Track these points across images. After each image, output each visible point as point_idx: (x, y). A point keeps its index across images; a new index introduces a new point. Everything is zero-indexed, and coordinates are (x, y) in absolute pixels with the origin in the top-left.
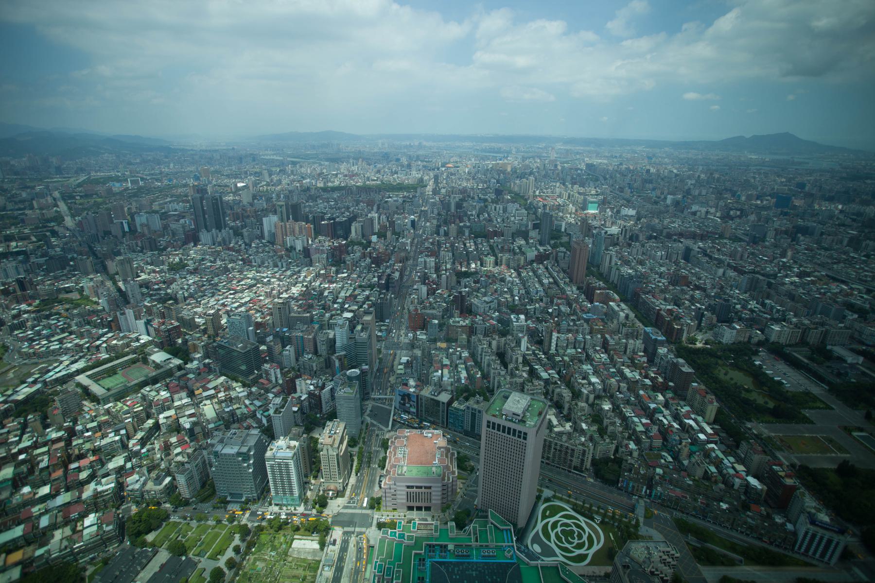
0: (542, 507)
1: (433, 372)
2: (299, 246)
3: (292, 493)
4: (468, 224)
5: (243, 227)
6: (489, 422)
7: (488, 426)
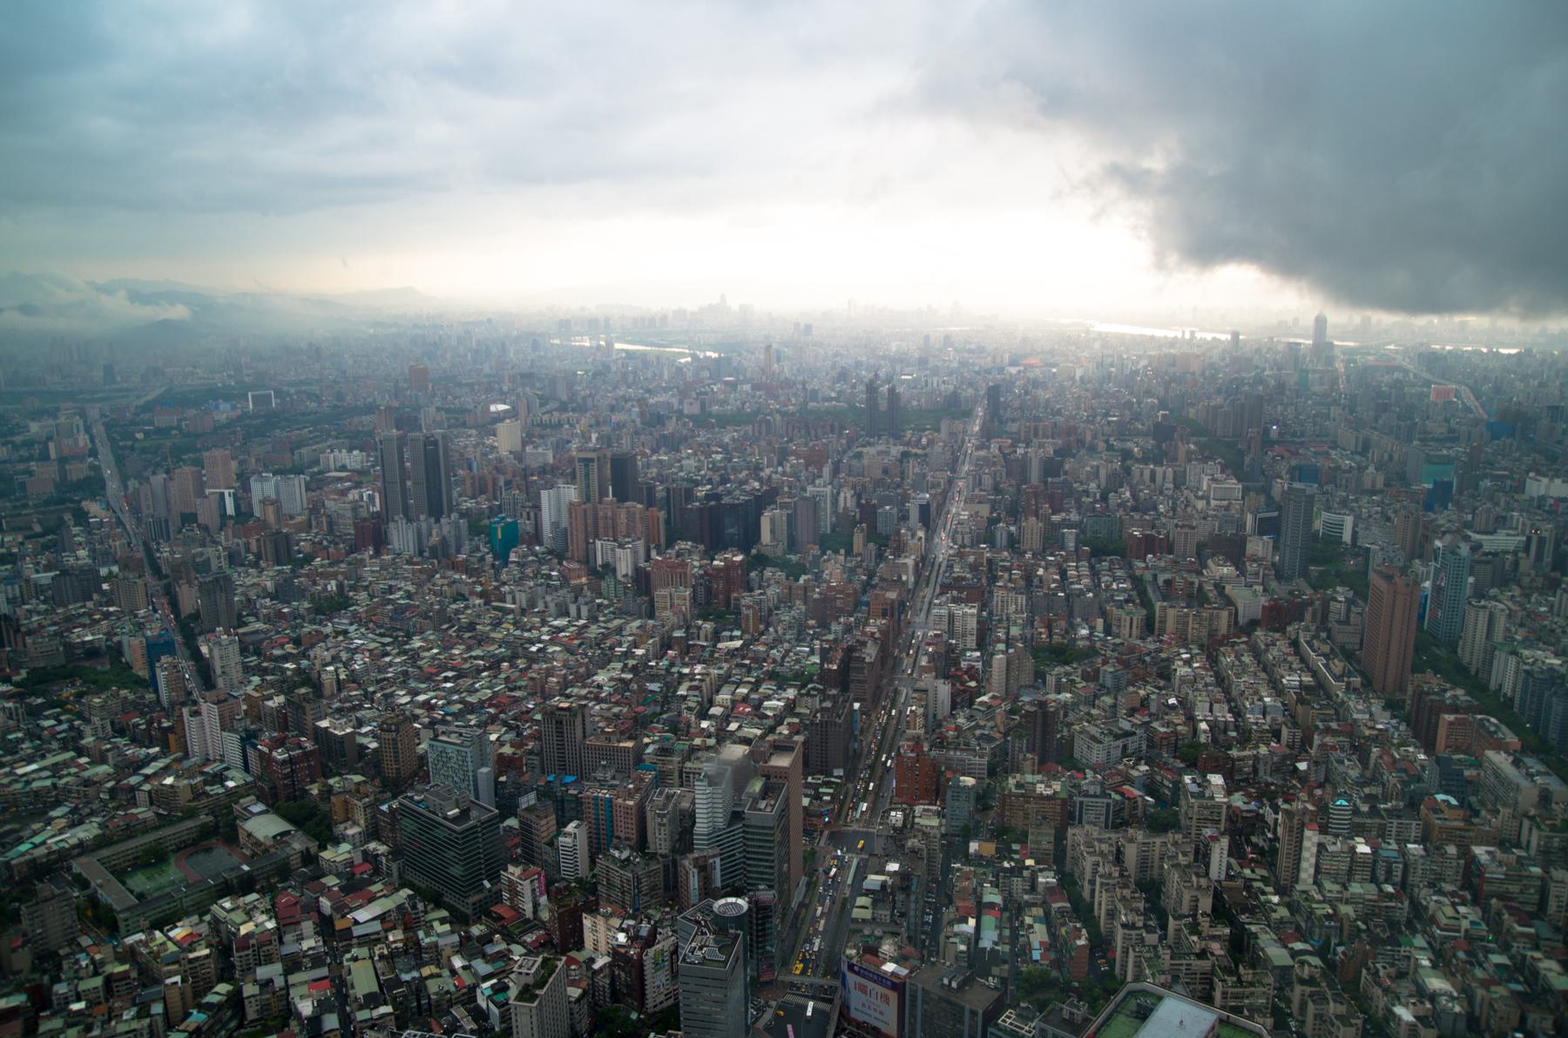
1: (951, 923)
2: (624, 567)
4: (1074, 517)
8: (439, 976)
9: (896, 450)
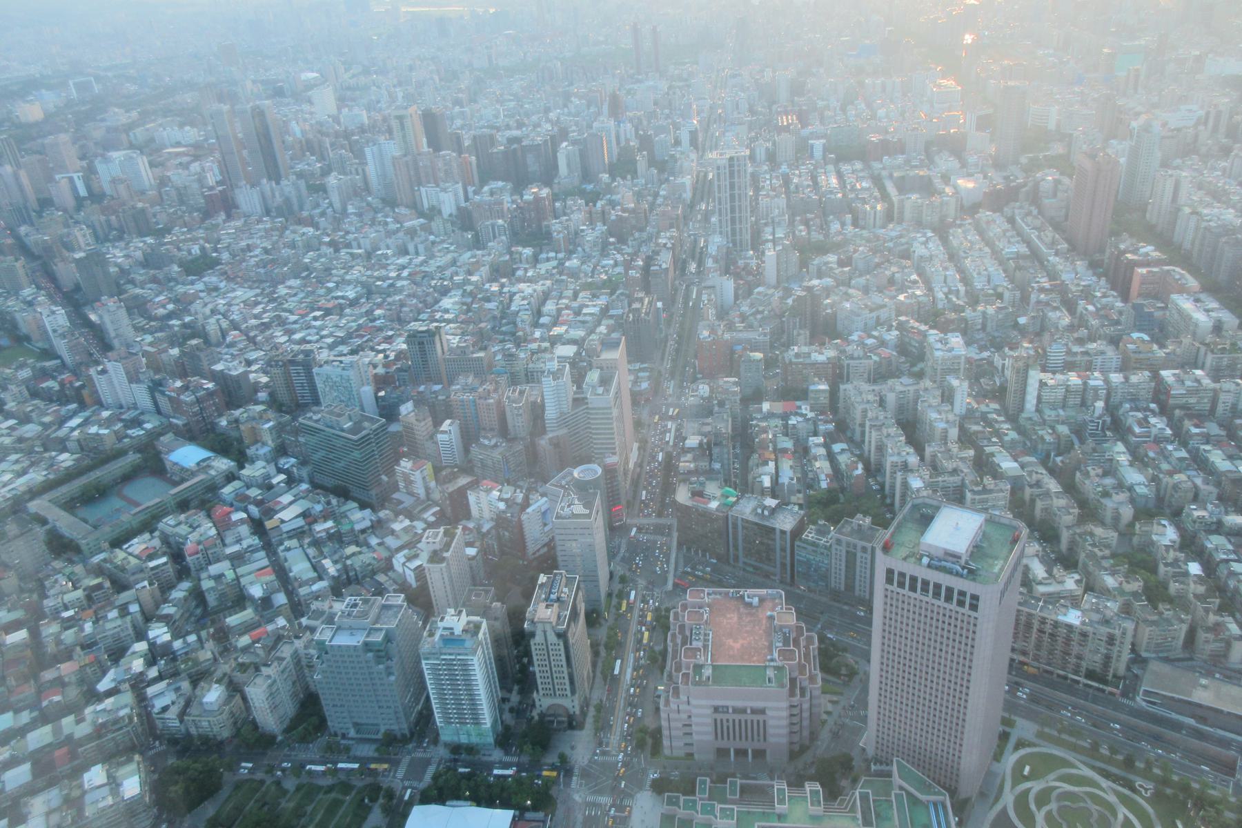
0: (1011, 758)
2: (448, 208)
3: (477, 721)
5: (326, 172)
6: (890, 572)
7: (889, 580)
8: (360, 553)
9: (663, 85)
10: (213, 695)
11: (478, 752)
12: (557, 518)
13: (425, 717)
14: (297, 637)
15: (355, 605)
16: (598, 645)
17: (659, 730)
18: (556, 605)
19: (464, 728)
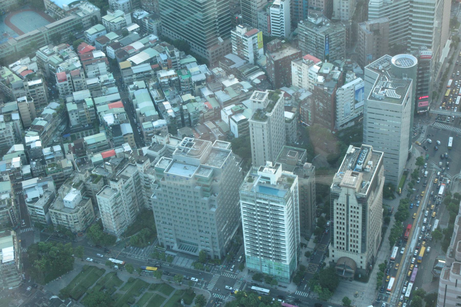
3: (278, 258)
8: (195, 101)
10: (71, 196)
11: (276, 283)
12: (371, 98)
13: (236, 246)
14: (141, 163)
15: (190, 145)
16: (390, 214)
17: (435, 296)
18: (361, 174)
19: (268, 261)
